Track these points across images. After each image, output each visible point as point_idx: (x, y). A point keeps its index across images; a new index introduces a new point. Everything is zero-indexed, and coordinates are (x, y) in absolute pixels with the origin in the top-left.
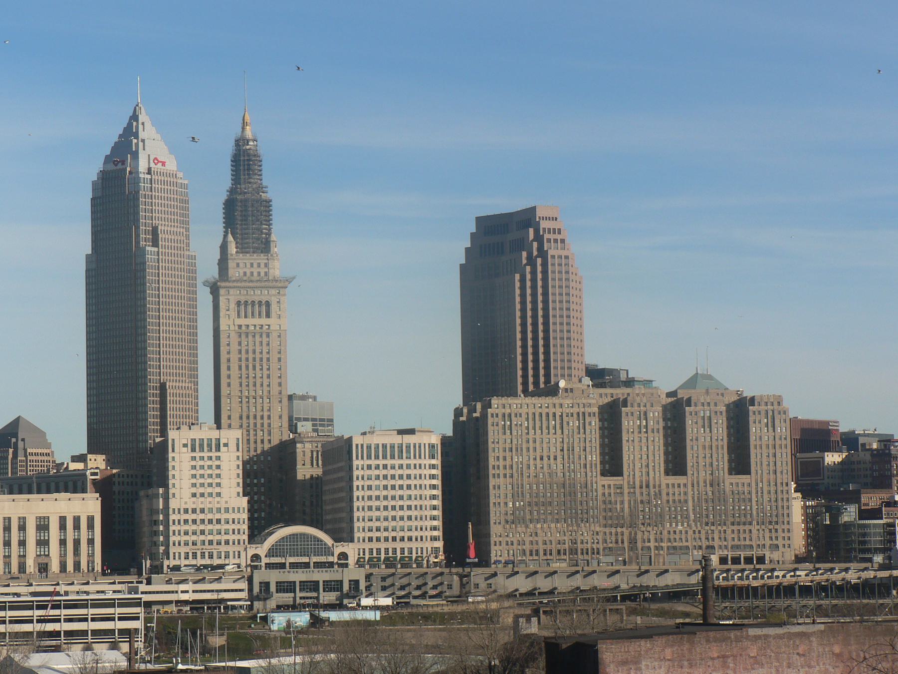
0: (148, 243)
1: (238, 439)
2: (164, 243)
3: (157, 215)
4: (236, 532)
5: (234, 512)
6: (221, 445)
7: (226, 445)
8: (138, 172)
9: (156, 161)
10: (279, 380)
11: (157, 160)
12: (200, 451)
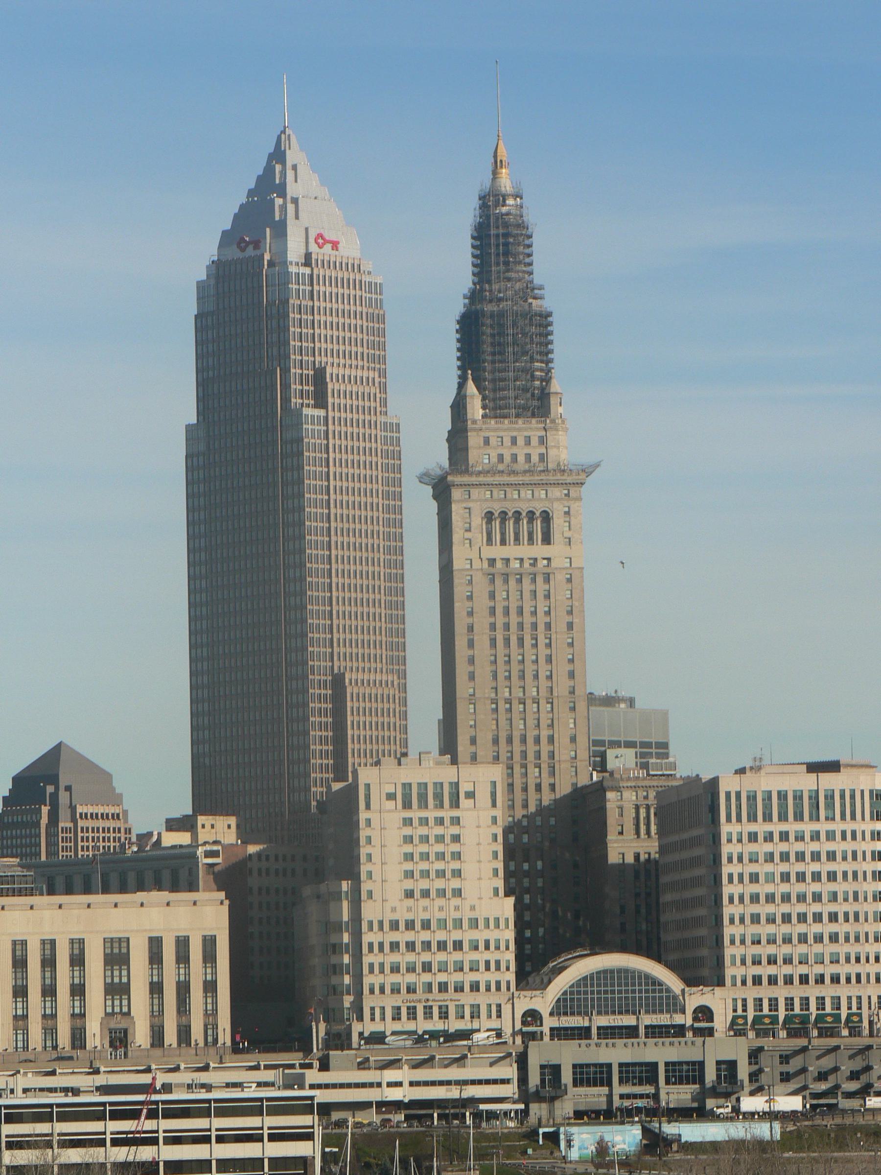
0: (306, 401)
1: (494, 784)
2: (337, 401)
3: (324, 346)
4: (493, 966)
5: (487, 926)
6: (462, 795)
7: (471, 795)
8: (285, 263)
9: (320, 241)
10: (570, 667)
12: (420, 807)
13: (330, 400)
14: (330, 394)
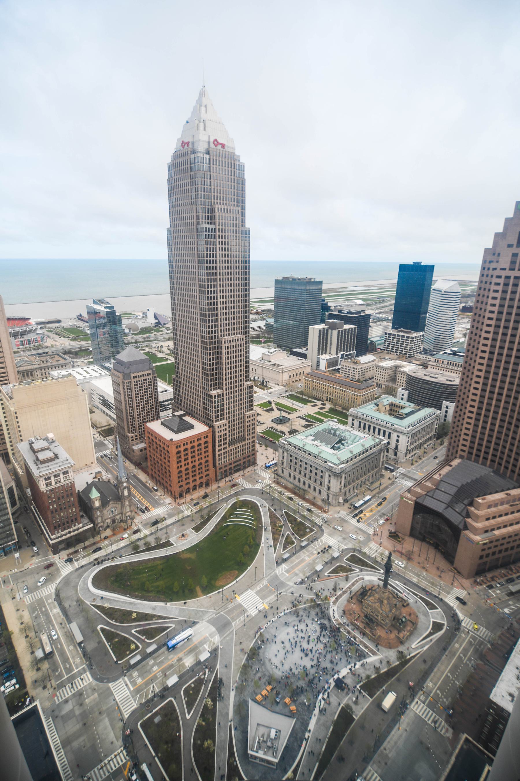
9: (216, 143)
11: (217, 142)
13: (217, 220)
14: (217, 218)
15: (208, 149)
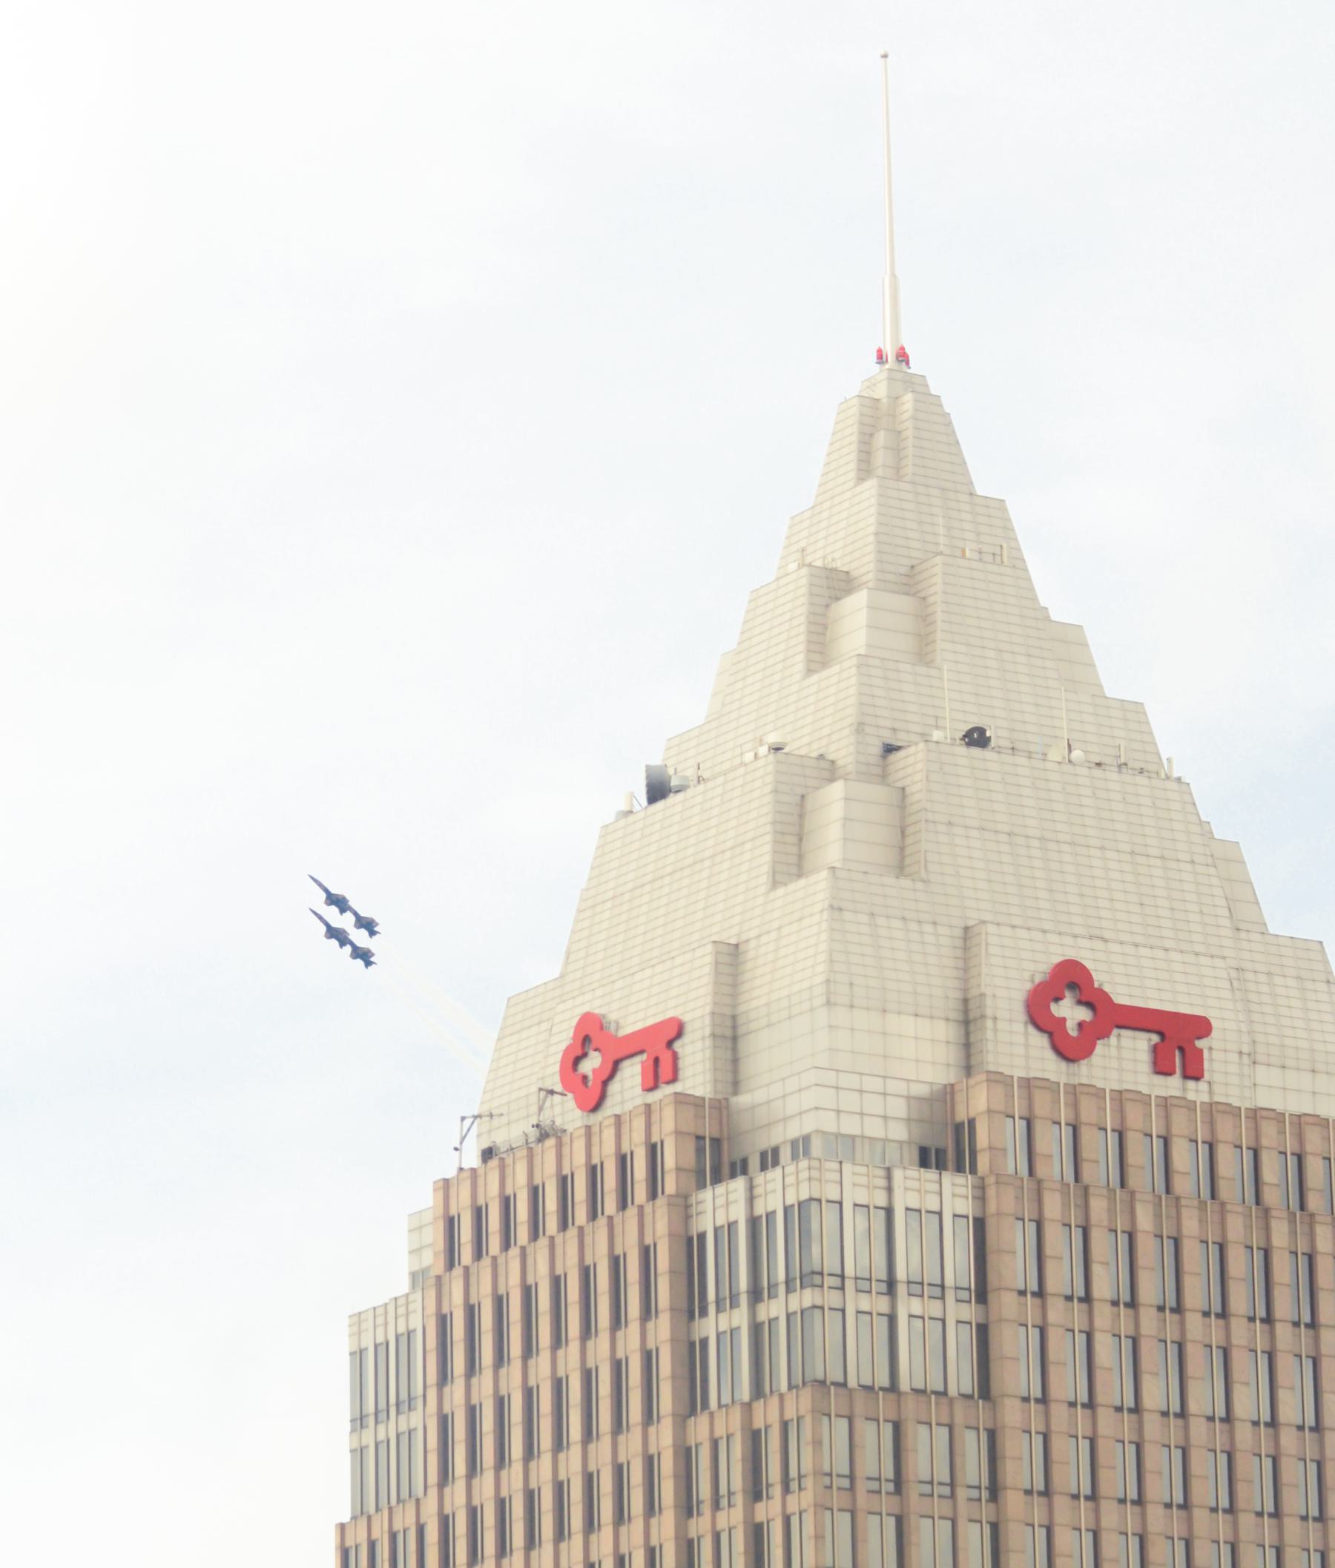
9: (1070, 1012)
15: (947, 1095)
